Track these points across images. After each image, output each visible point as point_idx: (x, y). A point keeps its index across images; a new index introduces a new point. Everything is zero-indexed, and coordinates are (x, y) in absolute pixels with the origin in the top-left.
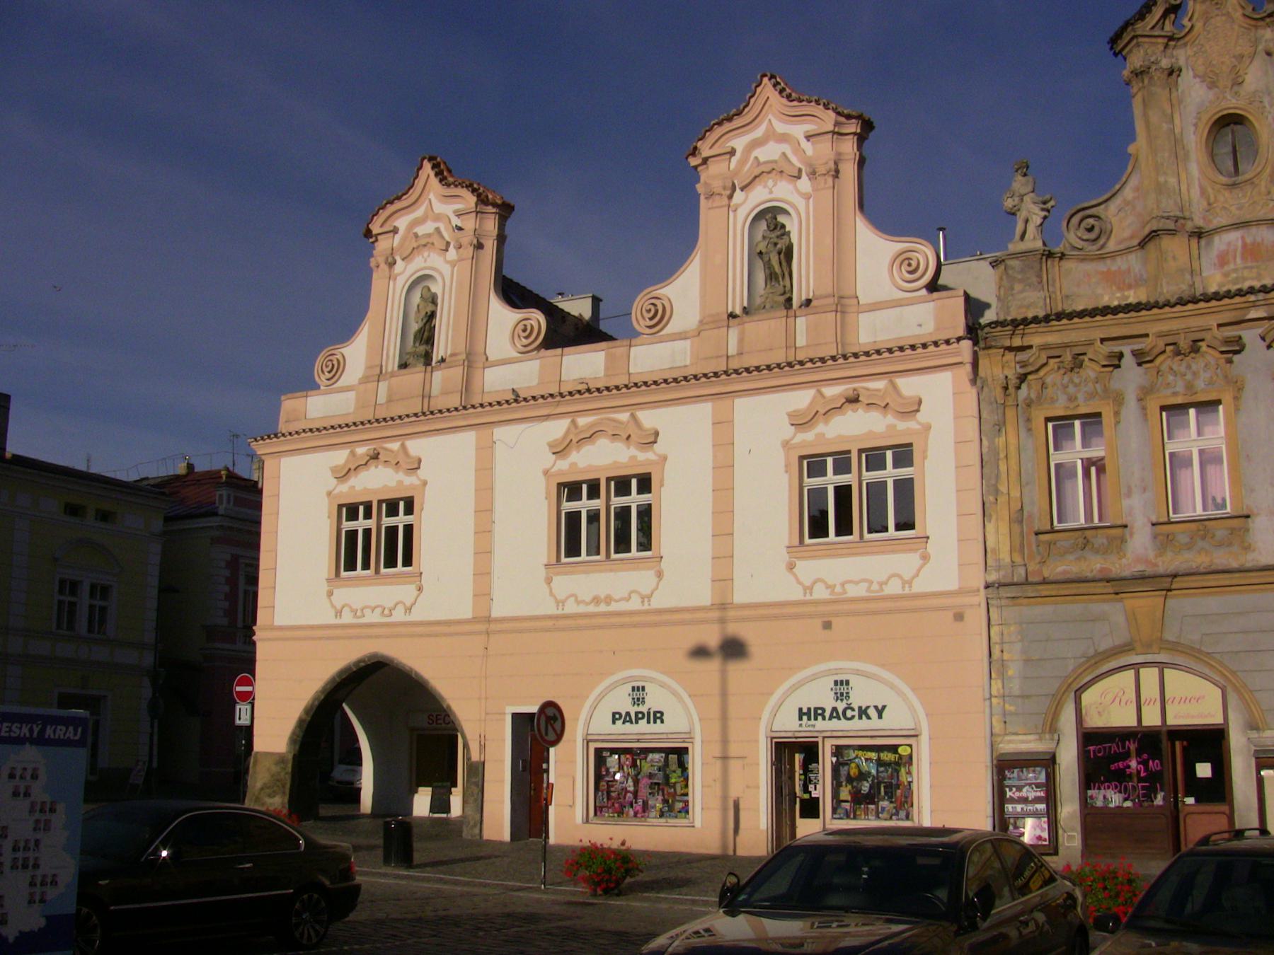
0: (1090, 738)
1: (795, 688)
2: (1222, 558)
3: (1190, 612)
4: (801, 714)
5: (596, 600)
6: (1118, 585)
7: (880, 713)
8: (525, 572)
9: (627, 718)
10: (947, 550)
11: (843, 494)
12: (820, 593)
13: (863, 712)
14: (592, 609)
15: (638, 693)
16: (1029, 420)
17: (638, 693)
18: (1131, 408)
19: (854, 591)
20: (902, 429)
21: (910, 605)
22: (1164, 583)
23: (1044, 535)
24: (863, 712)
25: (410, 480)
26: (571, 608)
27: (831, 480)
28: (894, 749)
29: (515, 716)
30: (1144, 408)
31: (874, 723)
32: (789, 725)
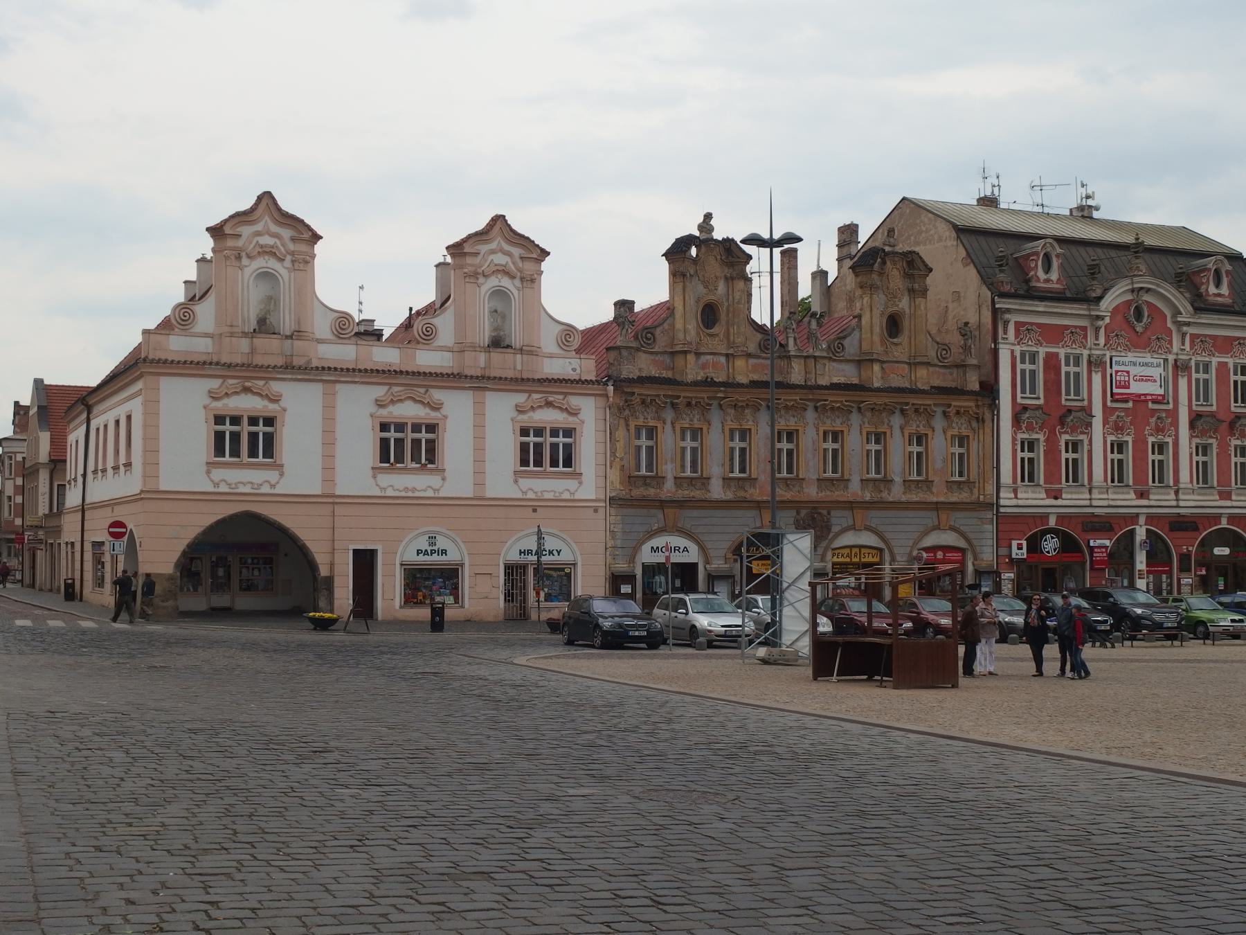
0: (646, 567)
1: (519, 539)
2: (698, 494)
3: (688, 518)
4: (521, 552)
5: (406, 489)
6: (662, 504)
7: (559, 553)
8: (357, 469)
9: (426, 553)
10: (591, 478)
11: (538, 447)
12: (531, 495)
13: (551, 552)
14: (403, 494)
15: (432, 540)
16: (627, 425)
17: (432, 540)
18: (668, 427)
19: (547, 496)
20: (570, 421)
21: (573, 505)
22: (682, 504)
23: (631, 480)
24: (551, 552)
25: (272, 406)
26: (390, 493)
27: (532, 439)
28: (563, 570)
29: (355, 551)
30: (674, 427)
31: (555, 558)
32: (514, 557)
